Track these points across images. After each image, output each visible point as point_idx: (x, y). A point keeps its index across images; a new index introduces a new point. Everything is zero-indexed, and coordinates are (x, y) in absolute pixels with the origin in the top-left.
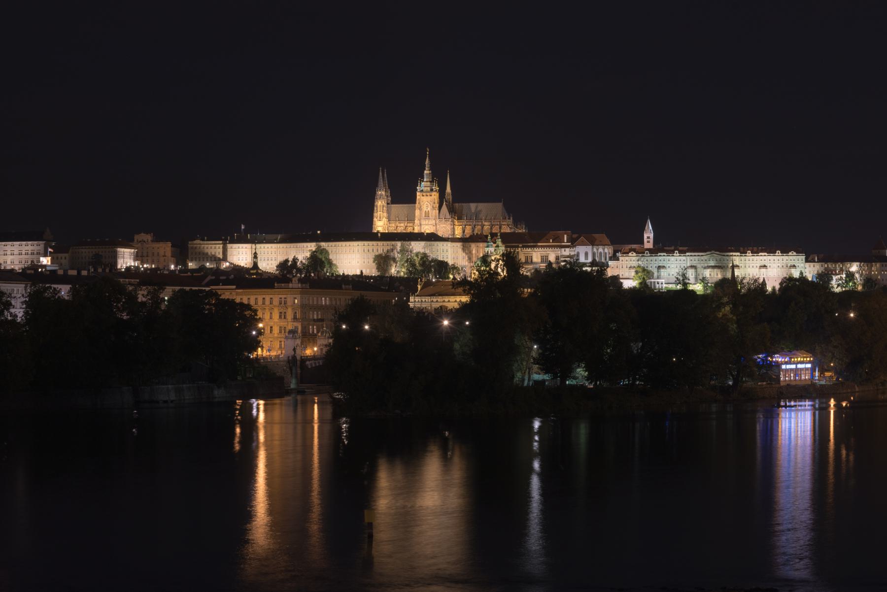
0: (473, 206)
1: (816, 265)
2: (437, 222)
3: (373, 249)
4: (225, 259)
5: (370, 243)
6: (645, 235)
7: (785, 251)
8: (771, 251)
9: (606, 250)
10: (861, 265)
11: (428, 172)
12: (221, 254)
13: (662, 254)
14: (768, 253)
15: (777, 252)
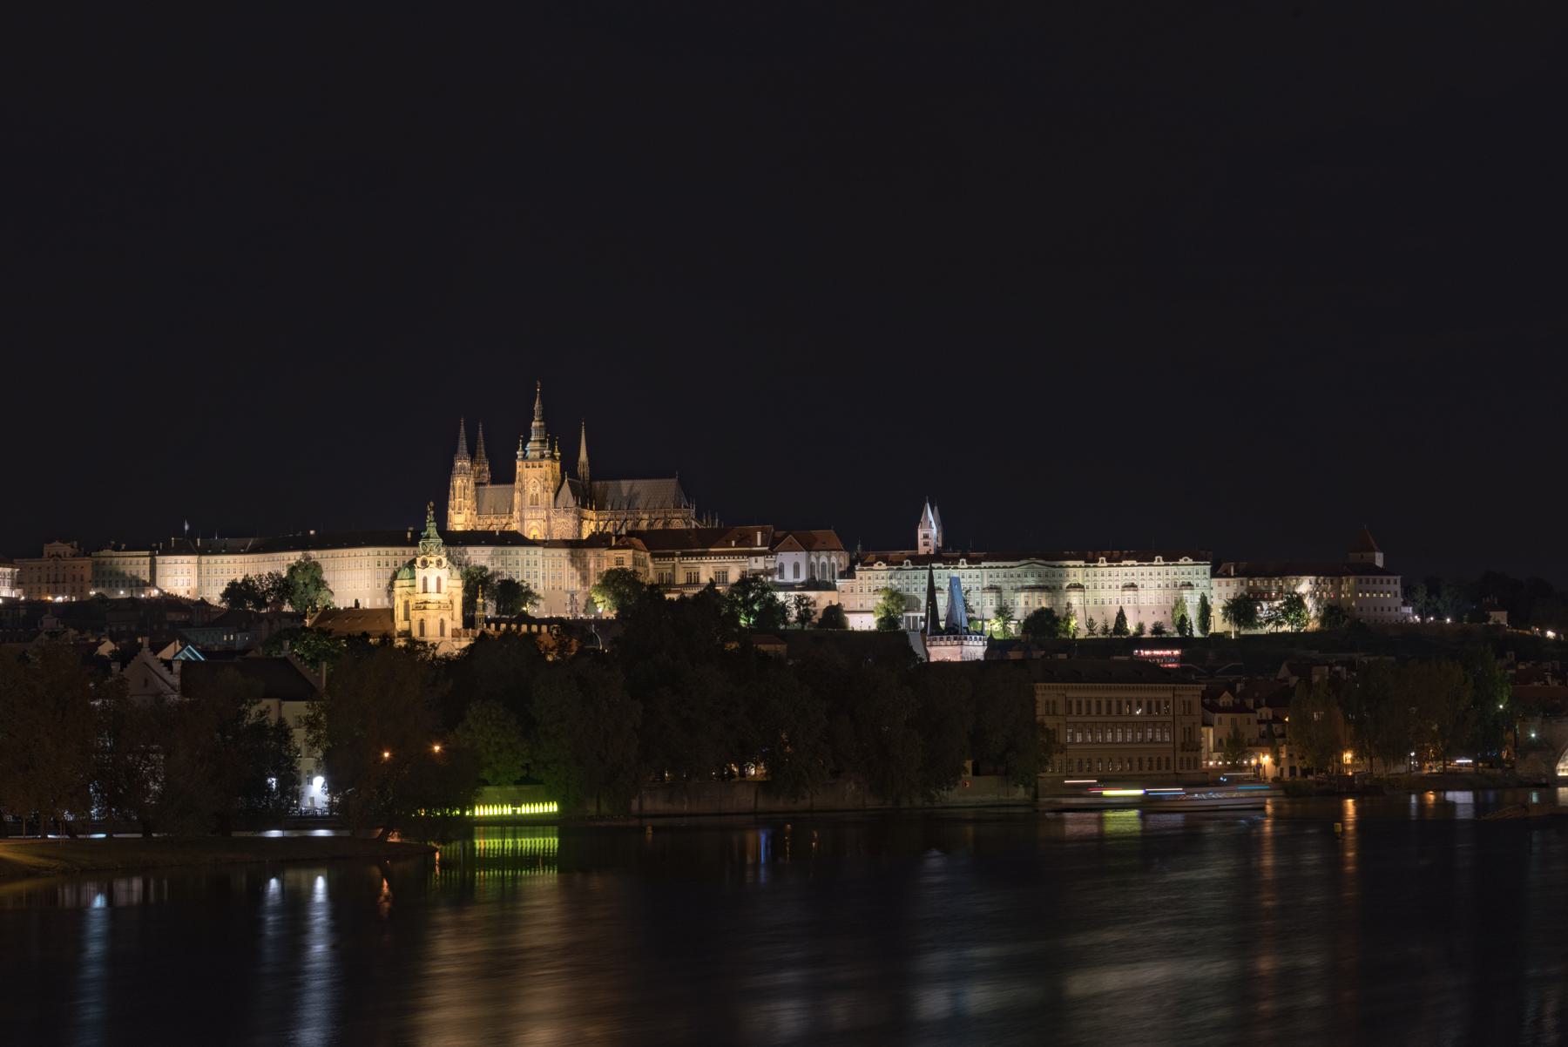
0: (625, 485)
1: (1231, 583)
2: (551, 514)
3: (396, 562)
4: (152, 583)
5: (391, 550)
6: (919, 531)
7: (1171, 557)
8: (1145, 557)
9: (834, 560)
10: (1320, 581)
11: (538, 424)
12: (148, 574)
14: (1138, 561)
15: (1157, 558)
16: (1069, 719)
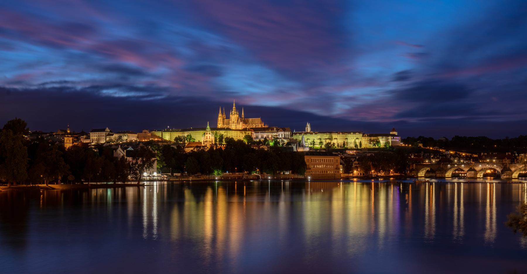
7: (354, 133)
13: (309, 134)
16: (312, 163)
